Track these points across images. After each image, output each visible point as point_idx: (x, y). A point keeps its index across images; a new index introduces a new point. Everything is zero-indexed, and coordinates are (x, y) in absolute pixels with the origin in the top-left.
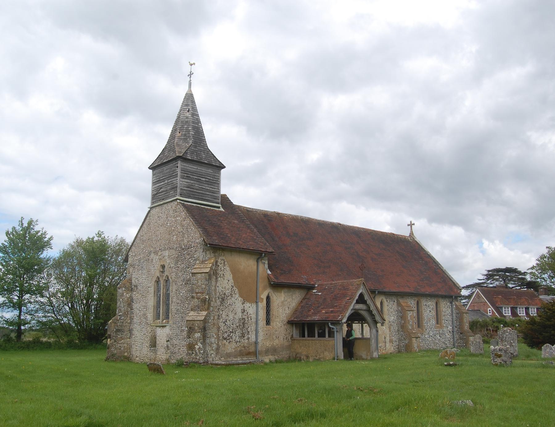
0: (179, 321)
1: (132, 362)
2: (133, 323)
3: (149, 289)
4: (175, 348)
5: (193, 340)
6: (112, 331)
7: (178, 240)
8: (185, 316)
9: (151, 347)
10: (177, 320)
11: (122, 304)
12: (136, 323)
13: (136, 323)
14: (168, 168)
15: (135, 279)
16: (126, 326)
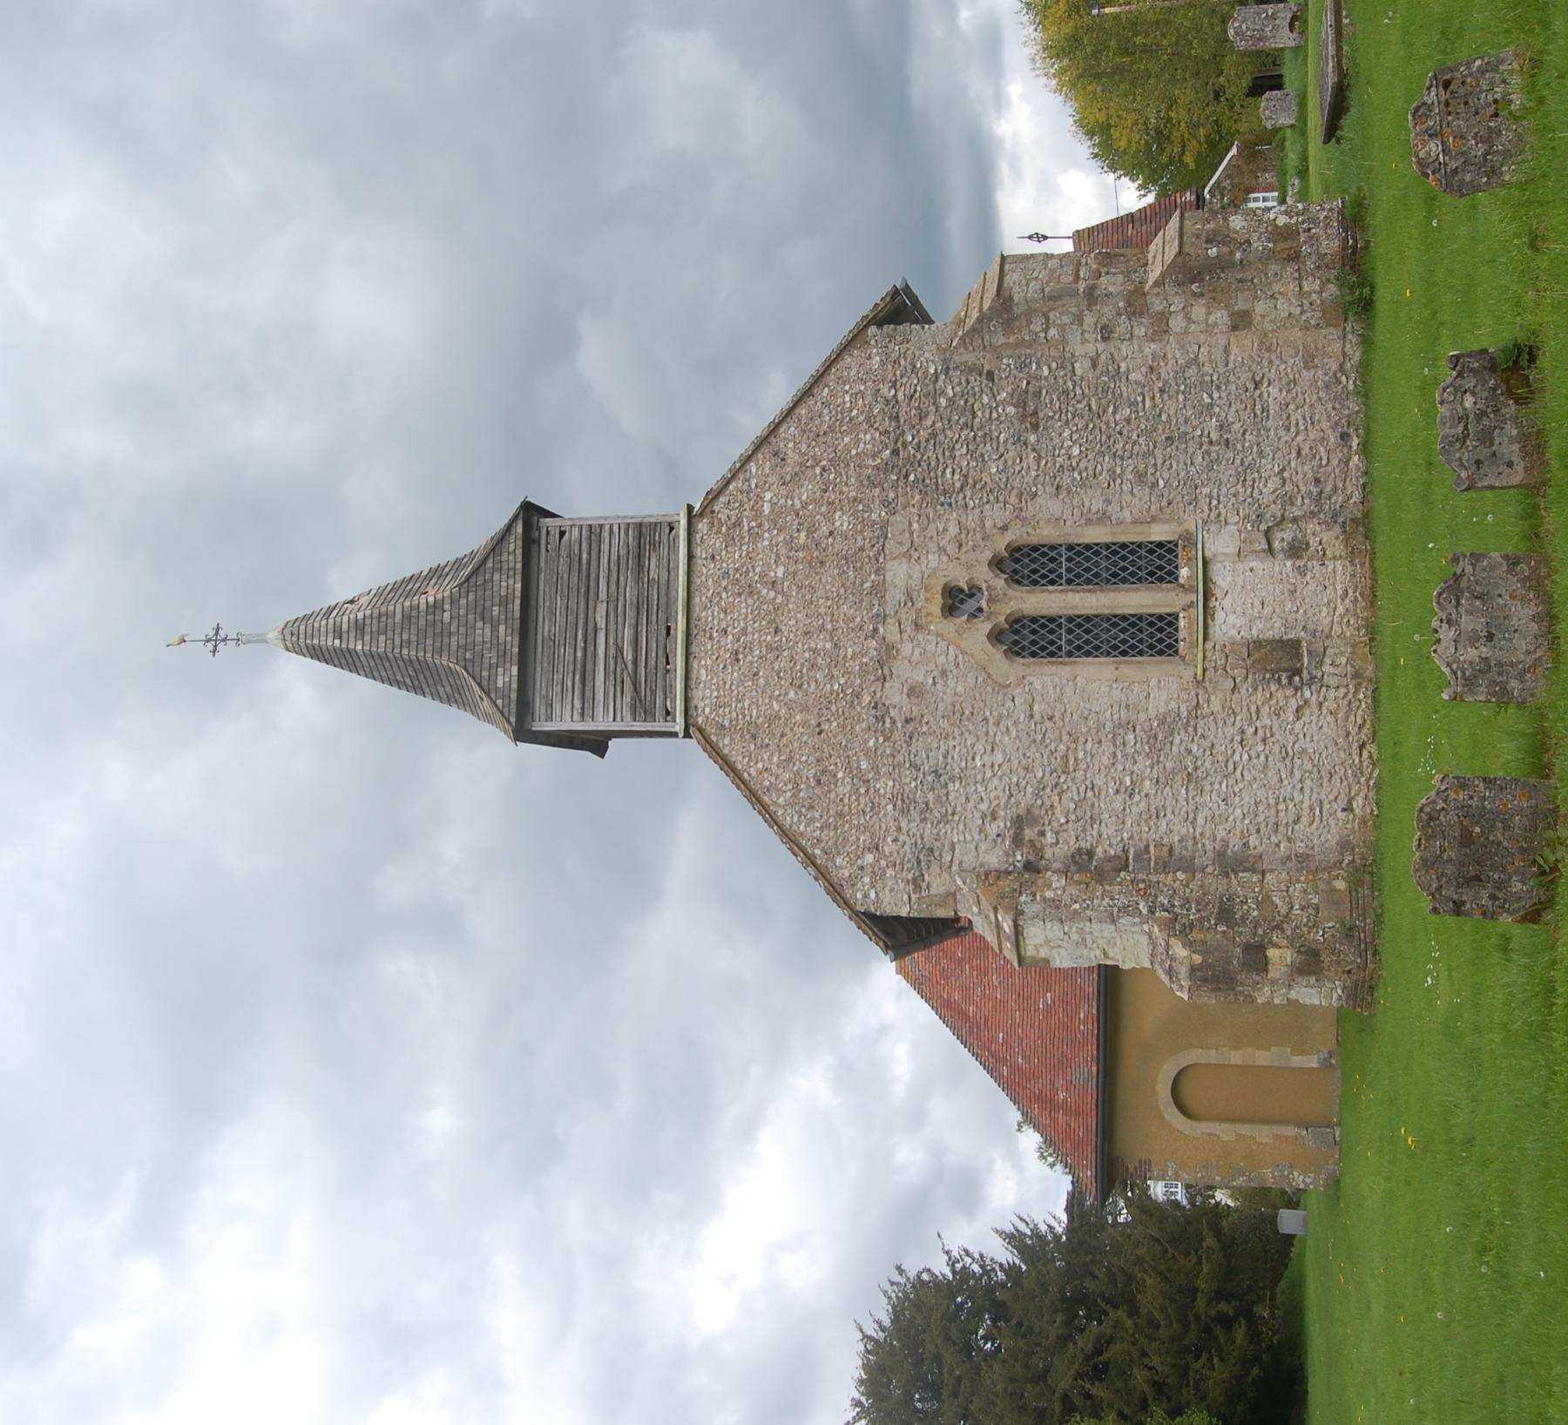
0: (1186, 464)
1: (1375, 847)
2: (1190, 844)
3: (1037, 717)
4: (1298, 487)
5: (1255, 231)
6: (1227, 939)
7: (855, 499)
8: (1164, 417)
9: (1298, 672)
10: (1182, 474)
11: (1095, 901)
12: (1191, 816)
13: (1191, 816)
14: (547, 604)
15: (983, 847)
16: (1202, 886)
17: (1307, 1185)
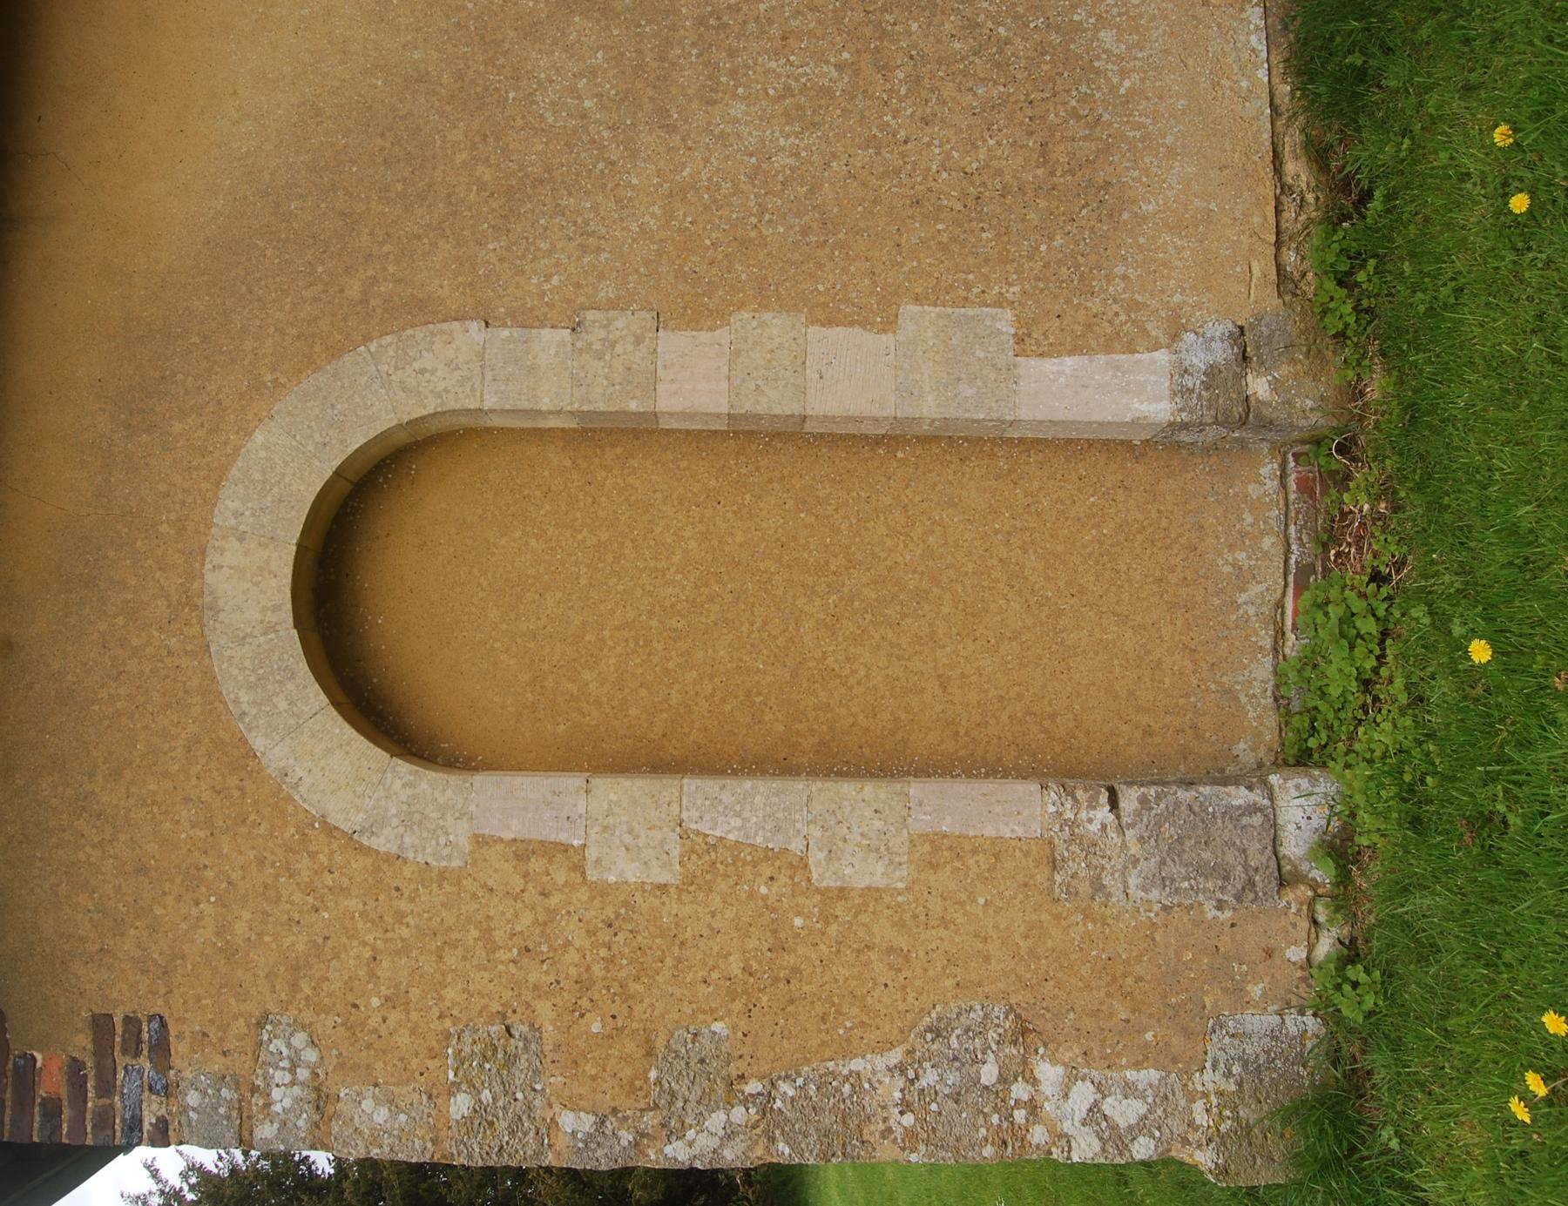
17: (1117, 1138)
